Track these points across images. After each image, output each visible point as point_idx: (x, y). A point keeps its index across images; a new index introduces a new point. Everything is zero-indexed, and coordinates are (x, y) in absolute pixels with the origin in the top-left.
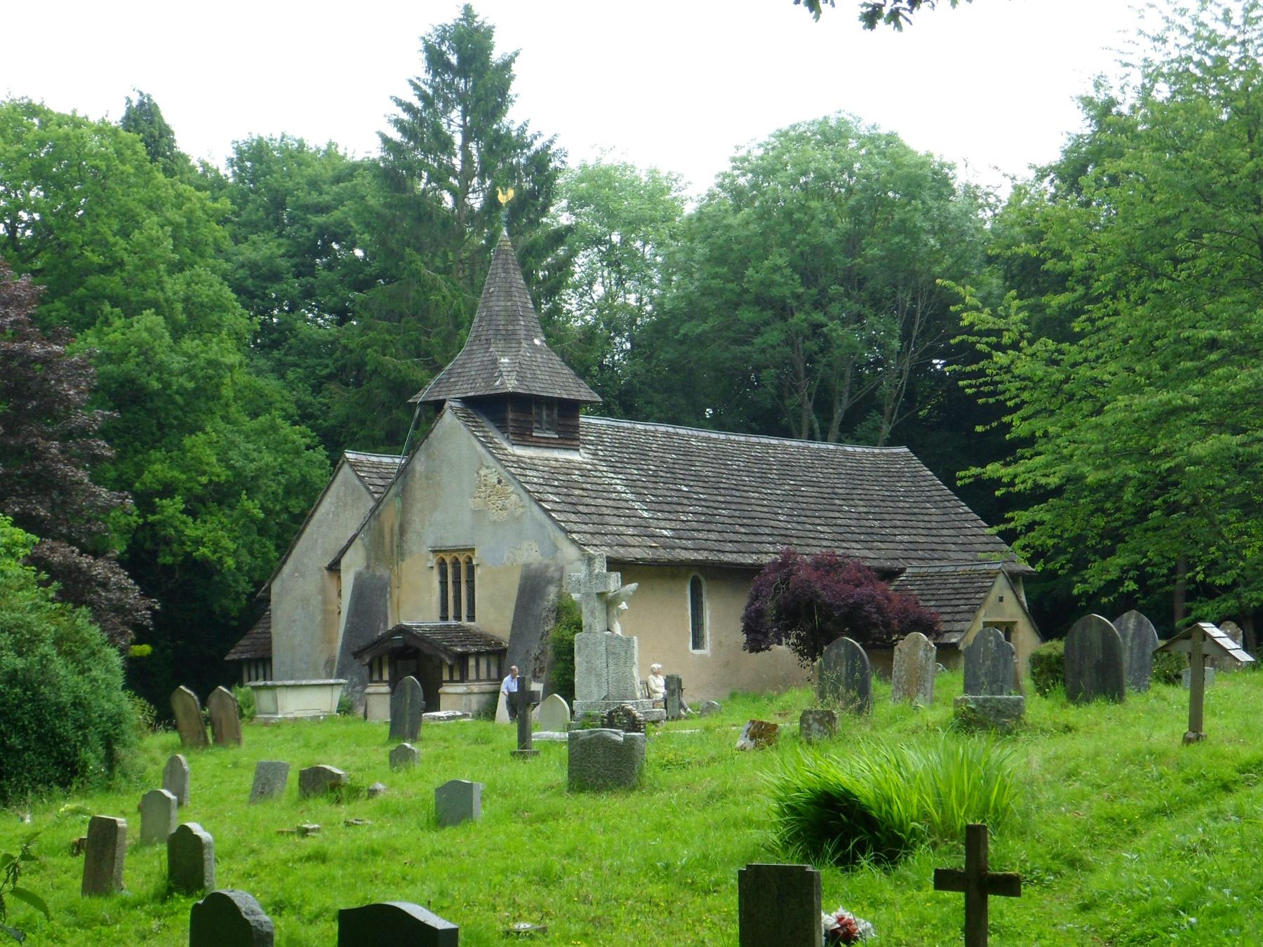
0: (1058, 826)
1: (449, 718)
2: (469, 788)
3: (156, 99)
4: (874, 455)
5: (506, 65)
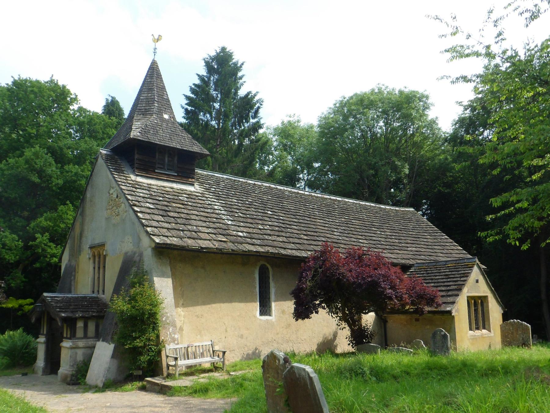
3: (118, 99)
4: (396, 210)
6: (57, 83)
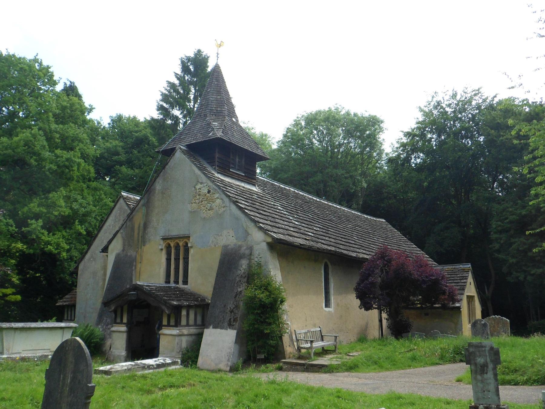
1: (159, 366)
3: (76, 84)
6: (41, 62)
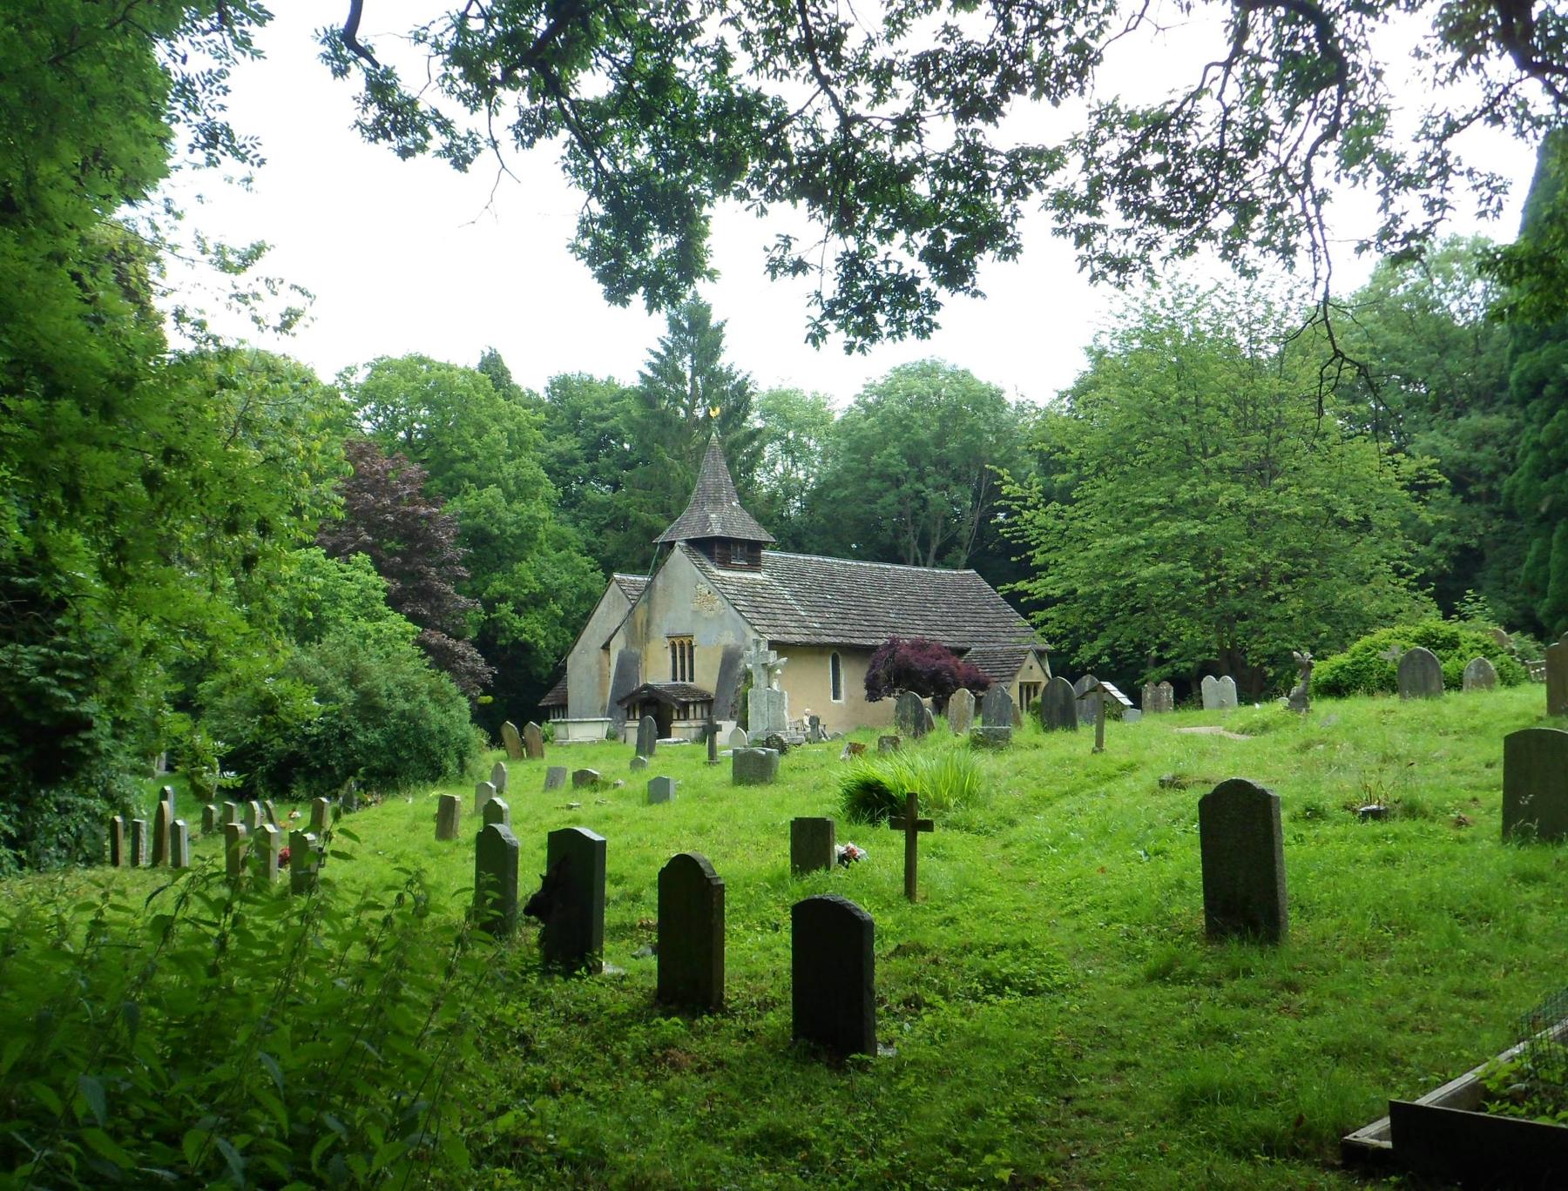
0: (1005, 802)
2: (667, 781)
5: (720, 328)
